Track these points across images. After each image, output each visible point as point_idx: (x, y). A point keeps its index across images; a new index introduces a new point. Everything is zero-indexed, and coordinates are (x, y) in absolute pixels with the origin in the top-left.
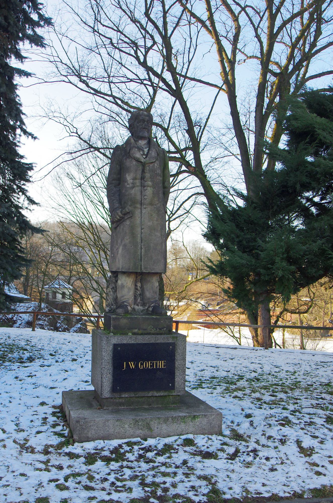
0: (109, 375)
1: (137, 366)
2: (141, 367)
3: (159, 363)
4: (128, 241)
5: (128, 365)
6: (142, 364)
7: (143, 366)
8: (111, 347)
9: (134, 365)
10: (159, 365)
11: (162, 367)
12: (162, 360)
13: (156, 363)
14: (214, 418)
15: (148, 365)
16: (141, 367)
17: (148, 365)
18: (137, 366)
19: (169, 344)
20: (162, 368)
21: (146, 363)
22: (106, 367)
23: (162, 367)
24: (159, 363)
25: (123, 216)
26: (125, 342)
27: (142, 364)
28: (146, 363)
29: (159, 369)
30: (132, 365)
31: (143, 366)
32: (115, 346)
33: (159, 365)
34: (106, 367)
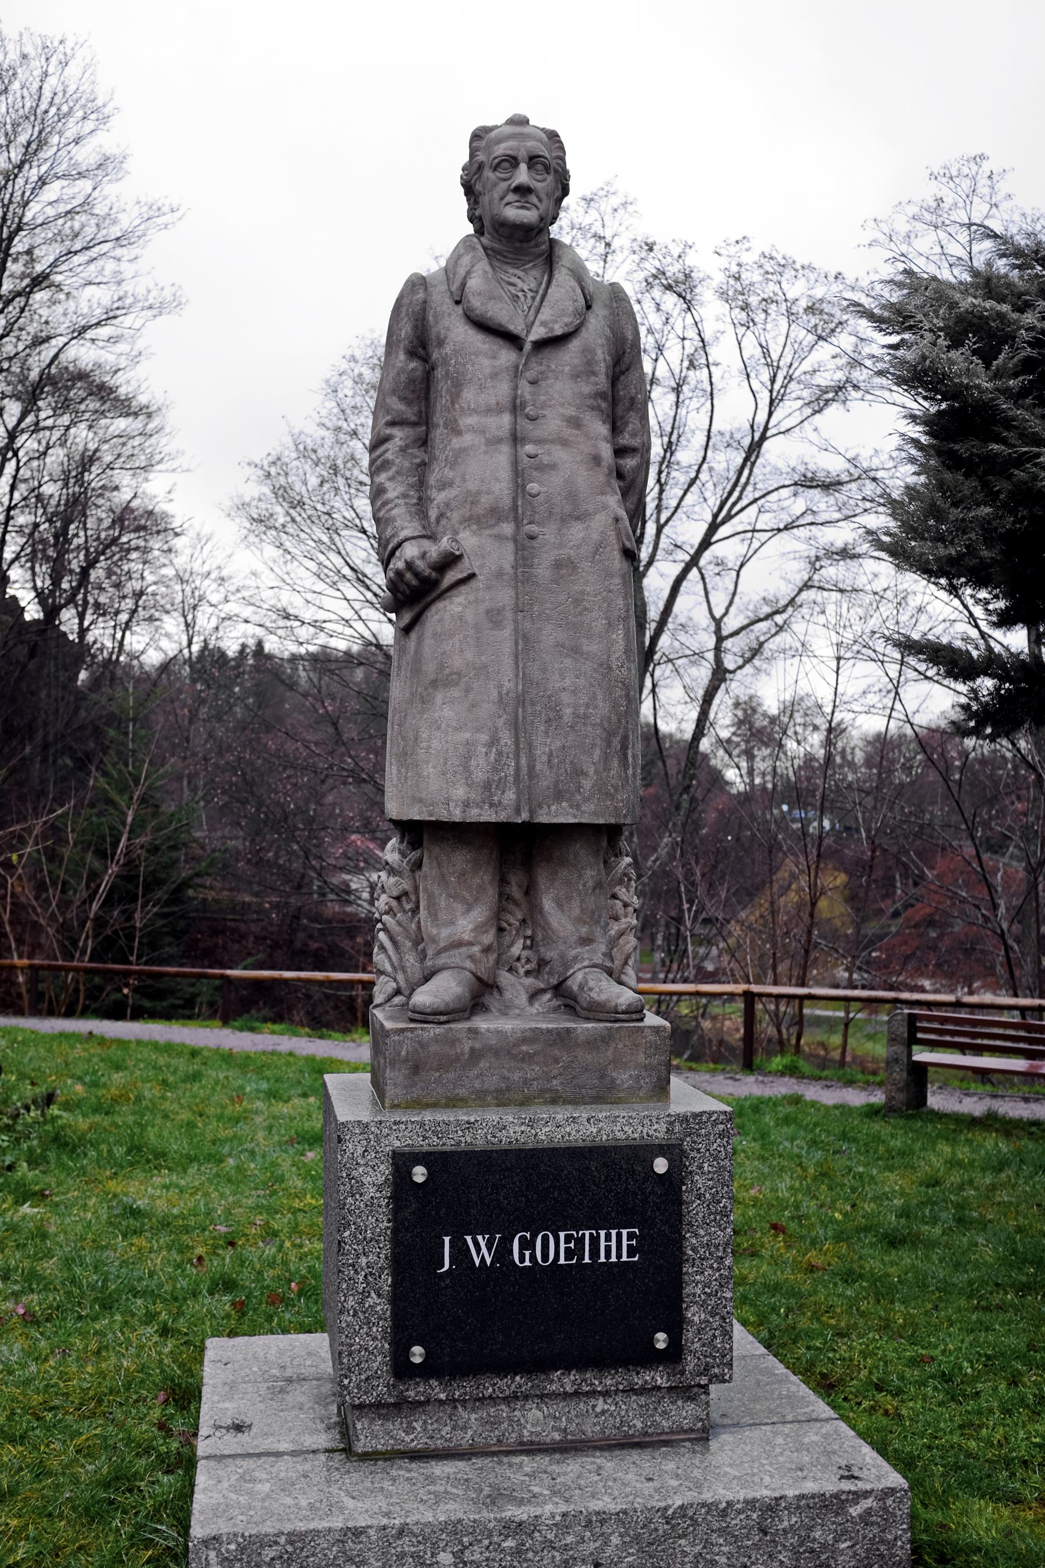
1: (503, 1253)
2: (522, 1260)
3: (608, 1238)
5: (460, 1253)
6: (527, 1245)
7: (533, 1257)
11: (619, 1255)
12: (619, 1226)
13: (595, 1241)
14: (868, 1512)
16: (522, 1260)
18: (503, 1253)
20: (619, 1264)
23: (619, 1255)
24: (608, 1238)
27: (527, 1245)
31: (533, 1257)
32: (402, 1162)
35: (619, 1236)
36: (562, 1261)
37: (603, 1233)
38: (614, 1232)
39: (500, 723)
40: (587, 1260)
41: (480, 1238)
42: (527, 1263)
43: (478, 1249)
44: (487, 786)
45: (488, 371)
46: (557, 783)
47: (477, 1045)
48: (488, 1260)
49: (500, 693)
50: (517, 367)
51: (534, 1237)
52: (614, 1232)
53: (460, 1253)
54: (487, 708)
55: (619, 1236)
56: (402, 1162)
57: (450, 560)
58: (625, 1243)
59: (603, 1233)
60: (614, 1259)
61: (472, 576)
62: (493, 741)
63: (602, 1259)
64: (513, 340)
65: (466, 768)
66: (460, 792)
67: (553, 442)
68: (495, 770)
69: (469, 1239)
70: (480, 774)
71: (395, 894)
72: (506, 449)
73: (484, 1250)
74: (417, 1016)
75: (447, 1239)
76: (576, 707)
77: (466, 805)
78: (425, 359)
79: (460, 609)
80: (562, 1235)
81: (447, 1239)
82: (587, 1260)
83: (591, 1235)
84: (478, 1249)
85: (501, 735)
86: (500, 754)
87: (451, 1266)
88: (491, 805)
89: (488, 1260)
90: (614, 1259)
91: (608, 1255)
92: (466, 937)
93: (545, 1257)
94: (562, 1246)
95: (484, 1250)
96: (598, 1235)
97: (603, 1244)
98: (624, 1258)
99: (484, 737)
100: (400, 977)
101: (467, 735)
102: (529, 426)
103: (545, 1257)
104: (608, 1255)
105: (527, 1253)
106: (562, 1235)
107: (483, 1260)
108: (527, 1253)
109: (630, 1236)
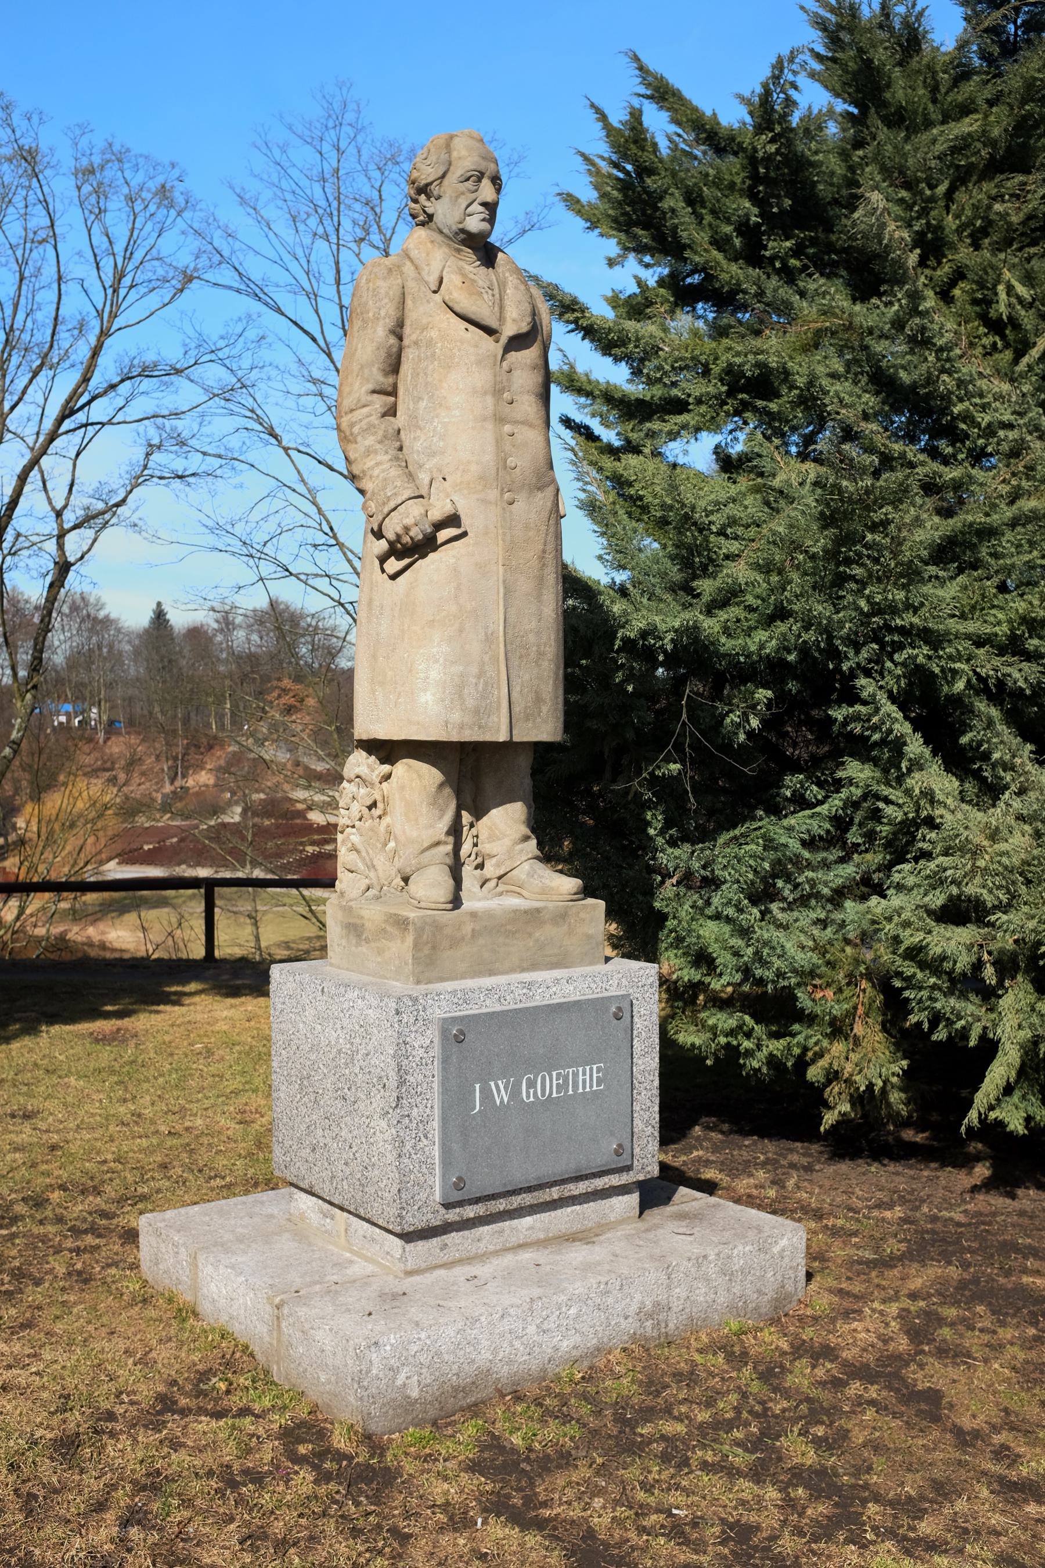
1: (515, 1093)
2: (528, 1097)
3: (584, 1074)
5: (487, 1094)
6: (531, 1084)
7: (535, 1093)
10: (584, 1081)
11: (591, 1086)
13: (575, 1075)
15: (548, 1084)
16: (528, 1097)
17: (548, 1084)
18: (515, 1093)
21: (543, 1079)
23: (591, 1086)
24: (584, 1074)
27: (531, 1084)
28: (543, 1079)
30: (501, 1094)
31: (535, 1093)
33: (584, 1081)
35: (591, 1070)
36: (554, 1095)
39: (486, 658)
40: (571, 1092)
43: (499, 1091)
44: (477, 711)
45: (473, 358)
46: (526, 708)
47: (478, 928)
48: (506, 1100)
49: (486, 634)
50: (495, 356)
51: (536, 1078)
53: (487, 1094)
54: (475, 647)
55: (591, 1070)
57: (453, 520)
58: (595, 1075)
61: (465, 534)
62: (481, 674)
64: (490, 331)
65: (461, 696)
66: (456, 717)
67: (523, 423)
68: (483, 697)
69: (492, 1084)
70: (470, 702)
71: (369, 803)
72: (490, 425)
73: (503, 1092)
74: (433, 906)
75: (477, 1086)
76: (538, 646)
77: (462, 727)
78: (400, 338)
79: (453, 561)
80: (554, 1074)
81: (477, 1086)
82: (571, 1092)
84: (499, 1091)
85: (487, 668)
86: (486, 684)
88: (480, 727)
89: (506, 1100)
91: (584, 1087)
92: (443, 837)
94: (555, 1082)
95: (503, 1092)
97: (581, 1078)
99: (474, 670)
100: (372, 874)
101: (461, 668)
102: (508, 409)
104: (584, 1087)
106: (554, 1074)
107: (502, 1101)
109: (599, 1070)
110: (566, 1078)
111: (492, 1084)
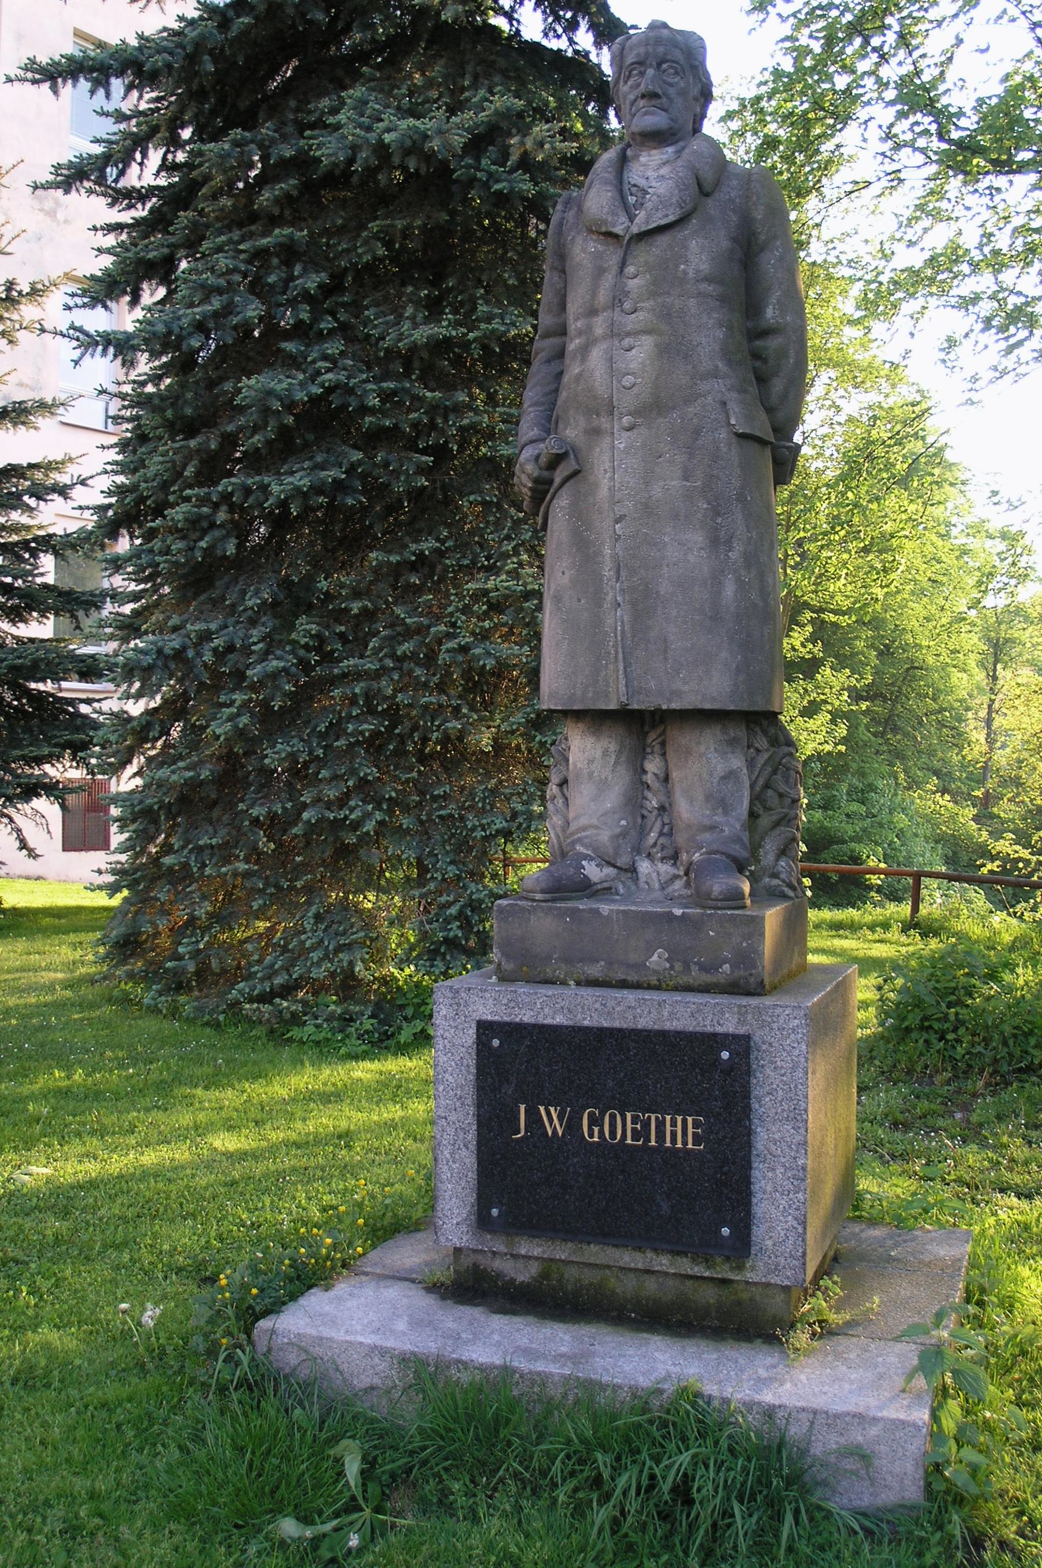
0: (464, 1152)
1: (573, 1126)
2: (591, 1136)
3: (674, 1124)
4: (565, 580)
7: (601, 1133)
8: (470, 1035)
9: (561, 1118)
10: (674, 1134)
11: (685, 1143)
12: (686, 1113)
13: (661, 1124)
16: (591, 1136)
18: (573, 1126)
19: (714, 1041)
21: (613, 1117)
22: (453, 1117)
23: (685, 1143)
24: (674, 1124)
25: (546, 474)
26: (527, 1017)
27: (594, 1121)
28: (613, 1117)
29: (674, 1151)
30: (553, 1122)
31: (601, 1133)
32: (485, 1029)
33: (674, 1134)
34: (453, 1117)
36: (629, 1141)
37: (668, 1118)
38: (679, 1119)
40: (653, 1143)
41: (552, 1109)
42: (596, 1139)
51: (602, 1114)
52: (679, 1119)
56: (485, 1029)
58: (690, 1130)
59: (668, 1118)
60: (679, 1145)
63: (668, 1144)
69: (542, 1109)
75: (522, 1107)
80: (629, 1115)
81: (522, 1107)
82: (653, 1143)
83: (657, 1118)
87: (526, 1132)
90: (679, 1145)
91: (674, 1140)
93: (613, 1133)
96: (664, 1119)
97: (668, 1128)
98: (690, 1146)
103: (613, 1133)
104: (674, 1140)
105: (596, 1129)
107: (555, 1130)
108: (596, 1129)
109: (696, 1125)
110: (646, 1124)
111: (542, 1109)
